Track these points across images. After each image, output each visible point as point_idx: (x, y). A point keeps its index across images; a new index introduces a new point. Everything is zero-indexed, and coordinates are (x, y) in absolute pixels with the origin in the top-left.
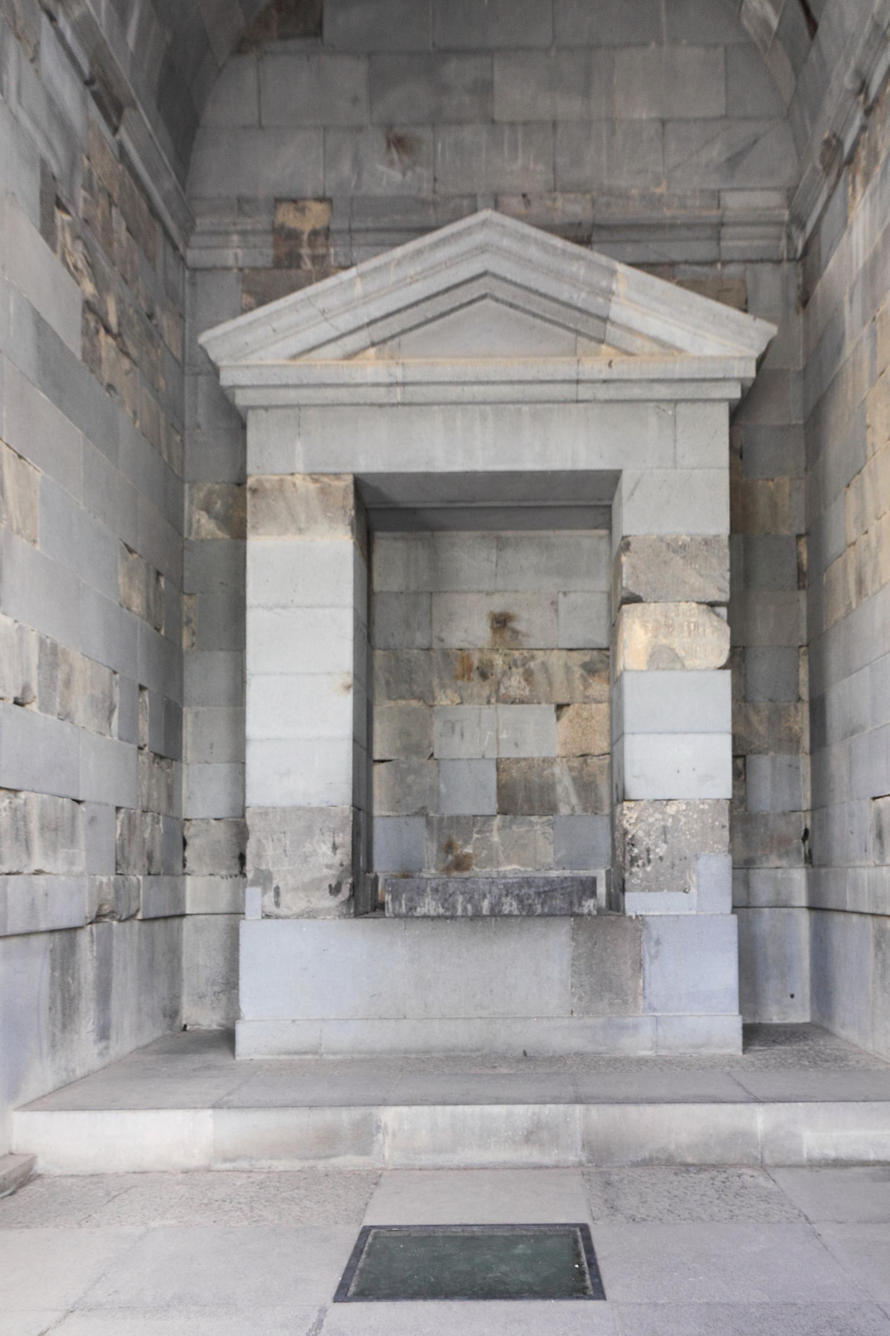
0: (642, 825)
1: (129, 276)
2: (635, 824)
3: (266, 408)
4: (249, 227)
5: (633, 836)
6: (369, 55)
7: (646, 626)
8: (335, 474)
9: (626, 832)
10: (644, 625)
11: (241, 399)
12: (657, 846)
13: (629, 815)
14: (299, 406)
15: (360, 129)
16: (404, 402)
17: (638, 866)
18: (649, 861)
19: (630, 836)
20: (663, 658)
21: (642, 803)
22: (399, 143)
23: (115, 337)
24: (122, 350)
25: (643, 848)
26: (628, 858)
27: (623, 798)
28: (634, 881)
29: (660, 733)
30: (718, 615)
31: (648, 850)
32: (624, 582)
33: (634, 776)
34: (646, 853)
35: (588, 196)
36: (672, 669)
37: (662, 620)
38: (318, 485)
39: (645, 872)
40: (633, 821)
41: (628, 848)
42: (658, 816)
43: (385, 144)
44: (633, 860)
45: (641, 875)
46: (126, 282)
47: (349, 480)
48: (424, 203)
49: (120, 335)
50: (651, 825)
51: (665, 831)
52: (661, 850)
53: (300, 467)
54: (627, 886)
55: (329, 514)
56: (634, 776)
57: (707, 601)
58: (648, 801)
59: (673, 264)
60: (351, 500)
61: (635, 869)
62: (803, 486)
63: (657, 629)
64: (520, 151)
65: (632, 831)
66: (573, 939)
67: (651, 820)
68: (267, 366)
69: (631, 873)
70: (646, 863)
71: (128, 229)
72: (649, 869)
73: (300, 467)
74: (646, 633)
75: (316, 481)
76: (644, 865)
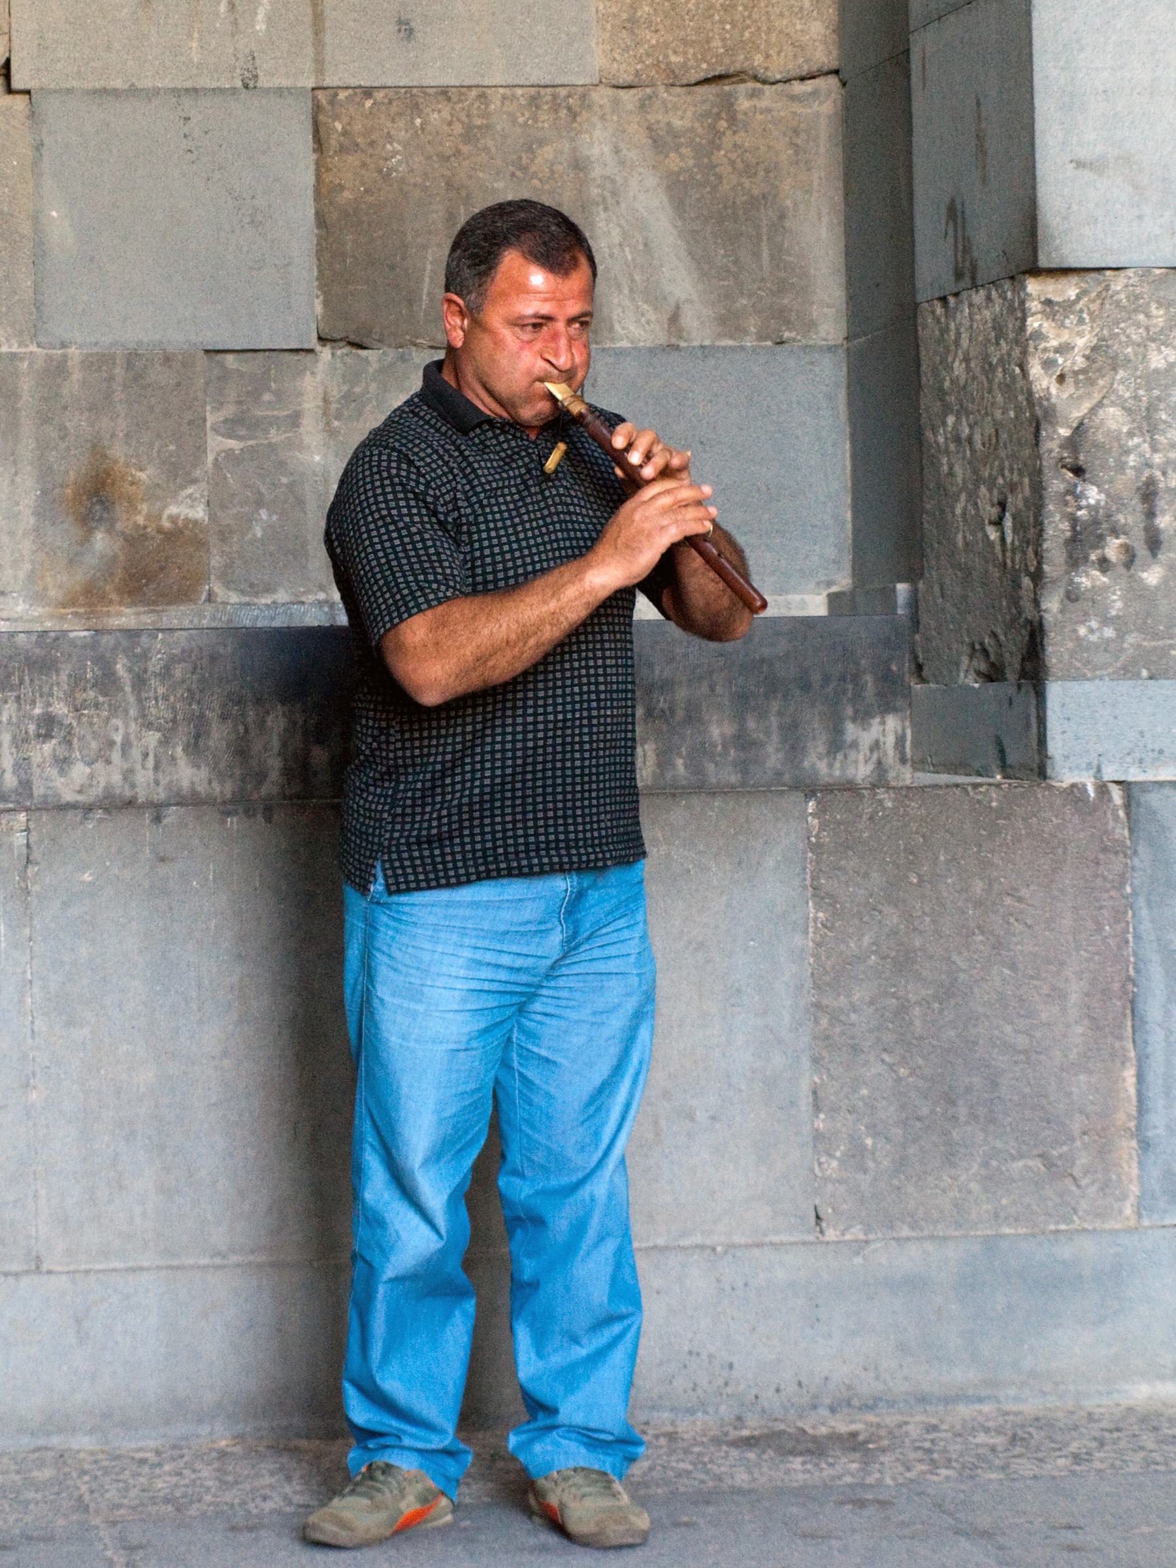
0: (1123, 384)
2: (1086, 377)
5: (1080, 429)
17: (1104, 564)
18: (1154, 543)
19: (1064, 432)
21: (1118, 284)
25: (1126, 481)
26: (1056, 528)
27: (1028, 260)
28: (1090, 630)
31: (1149, 494)
33: (1080, 164)
34: (1136, 503)
39: (1137, 591)
40: (1080, 362)
41: (1056, 484)
44: (1083, 540)
45: (1116, 604)
50: (1151, 379)
54: (1056, 651)
56: (1080, 164)
58: (1146, 271)
61: (1089, 579)
65: (1071, 407)
66: (820, 896)
69: (1072, 596)
70: (1142, 551)
72: (1152, 576)
76: (1130, 558)
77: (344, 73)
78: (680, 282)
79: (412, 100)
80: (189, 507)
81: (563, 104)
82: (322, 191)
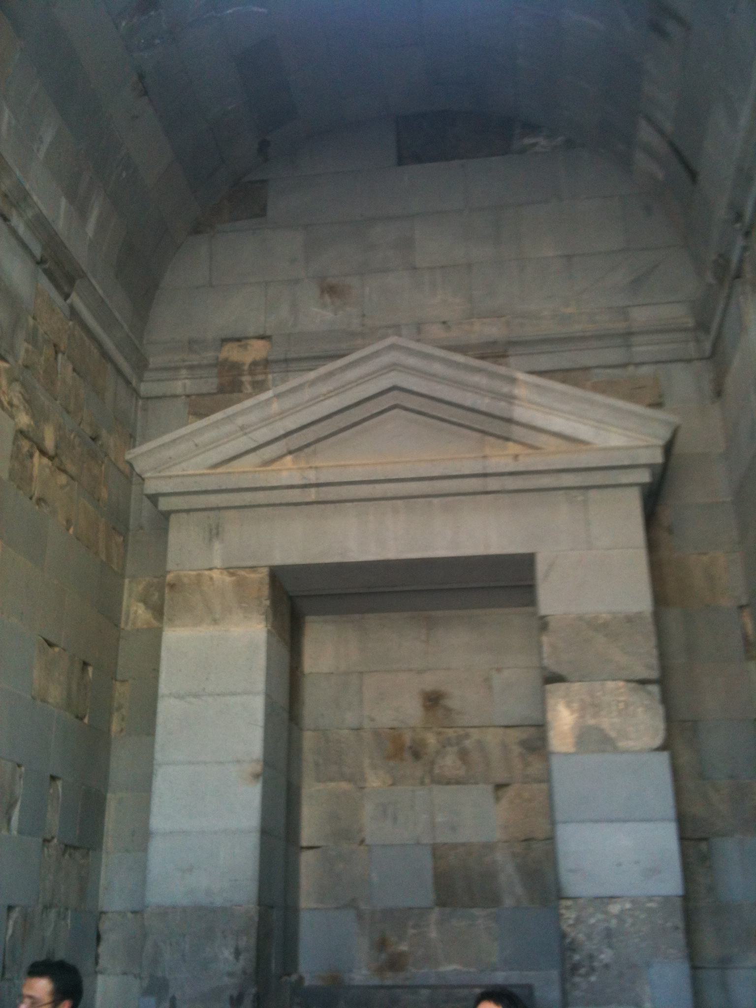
1: (72, 407)
3: (188, 511)
4: (195, 363)
9: (563, 936)
10: (568, 705)
11: (164, 504)
12: (602, 953)
13: (569, 915)
14: (219, 509)
16: (321, 498)
17: (581, 976)
18: (593, 970)
20: (592, 739)
21: (582, 901)
22: (332, 290)
23: (51, 458)
24: (59, 469)
28: (577, 993)
29: (596, 821)
30: (649, 693)
31: (591, 957)
35: (503, 319)
36: (604, 751)
38: (234, 578)
40: (571, 922)
42: (600, 916)
44: (575, 968)
46: (68, 412)
47: (265, 571)
49: (56, 455)
51: (609, 934)
52: (606, 956)
53: (217, 563)
55: (244, 605)
57: (637, 678)
59: (586, 369)
60: (266, 591)
61: (577, 979)
63: (583, 709)
67: (592, 921)
68: (190, 475)
71: (74, 370)
72: (593, 979)
73: (217, 563)
74: (573, 712)
75: (232, 574)
77: (441, 839)
78: (519, 890)
79: (454, 846)
80: (404, 947)
81: (489, 847)
82: (435, 868)
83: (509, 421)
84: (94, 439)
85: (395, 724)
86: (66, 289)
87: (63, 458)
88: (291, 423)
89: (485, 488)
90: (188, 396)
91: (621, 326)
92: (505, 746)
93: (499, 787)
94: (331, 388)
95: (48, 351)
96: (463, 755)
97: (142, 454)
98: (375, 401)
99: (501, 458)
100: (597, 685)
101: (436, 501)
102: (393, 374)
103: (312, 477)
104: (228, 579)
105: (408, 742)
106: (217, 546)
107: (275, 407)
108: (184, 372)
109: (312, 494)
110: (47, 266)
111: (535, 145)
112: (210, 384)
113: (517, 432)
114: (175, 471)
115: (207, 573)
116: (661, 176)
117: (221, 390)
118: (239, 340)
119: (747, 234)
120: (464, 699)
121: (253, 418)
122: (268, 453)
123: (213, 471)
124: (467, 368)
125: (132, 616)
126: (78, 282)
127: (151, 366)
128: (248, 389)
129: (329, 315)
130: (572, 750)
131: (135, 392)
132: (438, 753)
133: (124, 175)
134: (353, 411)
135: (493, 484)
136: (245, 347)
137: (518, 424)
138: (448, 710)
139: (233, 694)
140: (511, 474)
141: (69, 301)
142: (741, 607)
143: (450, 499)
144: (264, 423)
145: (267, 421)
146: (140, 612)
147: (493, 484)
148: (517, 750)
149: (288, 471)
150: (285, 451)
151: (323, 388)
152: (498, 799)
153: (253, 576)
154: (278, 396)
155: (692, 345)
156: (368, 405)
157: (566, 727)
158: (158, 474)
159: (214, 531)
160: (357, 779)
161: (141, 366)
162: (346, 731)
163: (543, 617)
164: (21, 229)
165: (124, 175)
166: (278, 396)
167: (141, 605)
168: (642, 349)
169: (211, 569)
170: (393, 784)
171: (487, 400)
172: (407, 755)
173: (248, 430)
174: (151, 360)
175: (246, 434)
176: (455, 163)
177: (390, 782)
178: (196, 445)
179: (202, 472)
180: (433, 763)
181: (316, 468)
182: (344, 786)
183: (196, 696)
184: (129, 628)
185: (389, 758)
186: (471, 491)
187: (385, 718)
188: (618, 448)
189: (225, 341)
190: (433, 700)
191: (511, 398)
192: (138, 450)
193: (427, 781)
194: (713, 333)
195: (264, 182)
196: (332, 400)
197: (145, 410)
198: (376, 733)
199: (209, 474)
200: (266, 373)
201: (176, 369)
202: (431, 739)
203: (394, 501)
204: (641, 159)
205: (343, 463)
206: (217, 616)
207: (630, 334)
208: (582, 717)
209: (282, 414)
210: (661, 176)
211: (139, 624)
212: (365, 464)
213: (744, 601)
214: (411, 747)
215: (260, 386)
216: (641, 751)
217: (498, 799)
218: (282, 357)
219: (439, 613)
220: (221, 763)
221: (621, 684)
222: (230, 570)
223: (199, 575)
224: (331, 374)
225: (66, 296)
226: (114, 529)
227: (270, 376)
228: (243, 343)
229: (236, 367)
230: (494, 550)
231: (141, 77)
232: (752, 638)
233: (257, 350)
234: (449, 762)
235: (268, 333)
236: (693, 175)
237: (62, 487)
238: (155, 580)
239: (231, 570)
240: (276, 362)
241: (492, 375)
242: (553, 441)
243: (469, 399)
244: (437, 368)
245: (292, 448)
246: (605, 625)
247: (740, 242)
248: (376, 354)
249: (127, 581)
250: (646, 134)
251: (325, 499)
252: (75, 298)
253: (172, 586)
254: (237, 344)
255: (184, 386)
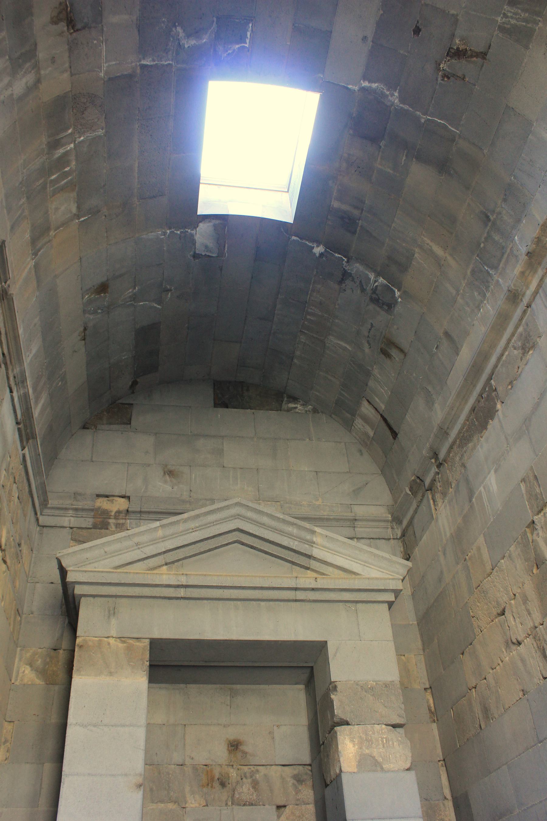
1: (14, 521)
3: (94, 596)
6: (156, 434)
7: (353, 741)
8: (138, 638)
10: (352, 741)
11: (78, 590)
14: (116, 596)
15: (149, 465)
22: (171, 473)
32: (335, 711)
37: (364, 736)
38: (125, 645)
43: (162, 473)
47: (147, 642)
48: (184, 502)
62: (423, 659)
64: (239, 481)
71: (18, 497)
73: (114, 633)
74: (354, 746)
75: (124, 642)
83: (309, 557)
84: (19, 545)
85: (208, 762)
86: (25, 443)
87: (7, 552)
88: (169, 545)
89: (294, 597)
90: (71, 528)
91: (350, 515)
92: (283, 778)
93: (279, 807)
94: (197, 525)
95: (12, 480)
96: (255, 784)
97: (68, 554)
98: (223, 536)
99: (306, 579)
100: (369, 726)
101: (263, 603)
102: (236, 520)
103: (183, 580)
104: (121, 645)
105: (217, 776)
106: (113, 621)
107: (160, 533)
108: (71, 512)
109: (182, 592)
110: (20, 426)
111: (296, 408)
112: (88, 522)
113: (314, 564)
114: (89, 568)
115: (106, 639)
116: (371, 434)
117: (95, 526)
118: (107, 496)
119: (439, 465)
120: (257, 746)
121: (144, 538)
122: (152, 562)
123: (115, 571)
124: (284, 521)
125: (21, 675)
126: (31, 441)
127: (49, 506)
128: (113, 528)
129: (168, 488)
130: (356, 770)
131: (37, 520)
132: (238, 783)
133: (60, 384)
134: (209, 541)
135: (300, 595)
136: (112, 501)
137: (315, 559)
138: (245, 753)
139: (123, 726)
140: (313, 589)
141: (23, 452)
142: (425, 689)
143: (271, 603)
144: (152, 543)
145: (154, 541)
146: (27, 672)
147: (300, 595)
148: (291, 782)
149: (166, 576)
150: (164, 563)
151: (192, 524)
152: (279, 817)
153: (138, 644)
154: (162, 526)
155: (390, 530)
156: (221, 538)
157: (351, 755)
158: (77, 569)
159: (112, 612)
160: (180, 802)
161: (44, 503)
162: (173, 766)
163: (331, 683)
164: (16, 400)
165: (60, 384)
166: (162, 526)
167: (28, 667)
168: (361, 531)
169: (108, 637)
170: (207, 805)
171: (296, 543)
172: (216, 784)
173: (140, 546)
174: (50, 501)
175: (139, 548)
176: (249, 411)
177: (205, 804)
178: (106, 552)
179: (108, 570)
180: (234, 791)
181: (186, 575)
182: (171, 806)
183: (95, 726)
184: (17, 683)
185: (203, 786)
186: (286, 598)
187: (201, 757)
188: (377, 579)
189: (98, 496)
190: (234, 746)
191: (312, 543)
192: (65, 551)
193: (230, 803)
194: (405, 523)
195: (132, 404)
196: (197, 533)
197: (41, 534)
198: (195, 768)
199: (113, 572)
200: (125, 519)
201: (66, 509)
202: (233, 774)
203: (235, 602)
204: (359, 423)
205: (205, 573)
206: (113, 670)
207: (356, 520)
208: (361, 748)
209: (164, 538)
210: (371, 434)
211: (26, 681)
212: (218, 575)
213: (427, 686)
214: (218, 779)
215: (120, 527)
216: (398, 770)
217: (279, 817)
218: (139, 510)
219: (238, 687)
220: (113, 775)
221: (384, 726)
222: (121, 639)
223: (100, 640)
224: (197, 516)
225: (23, 448)
226: (18, 611)
227: (128, 521)
228: (111, 498)
229: (105, 513)
230: (301, 638)
231: (85, 329)
232: (433, 709)
233: (121, 504)
234: (245, 790)
235: (127, 495)
236: (395, 435)
237: (4, 572)
238: (40, 650)
239: (122, 639)
240: (134, 512)
241: (300, 527)
242: (337, 571)
243: (285, 541)
244: (265, 520)
245: (168, 561)
246: (372, 688)
247: (434, 469)
248: (228, 507)
249: (19, 649)
250: (366, 409)
251: (190, 596)
252: (26, 451)
253: (81, 647)
254: (107, 499)
255: (70, 521)
